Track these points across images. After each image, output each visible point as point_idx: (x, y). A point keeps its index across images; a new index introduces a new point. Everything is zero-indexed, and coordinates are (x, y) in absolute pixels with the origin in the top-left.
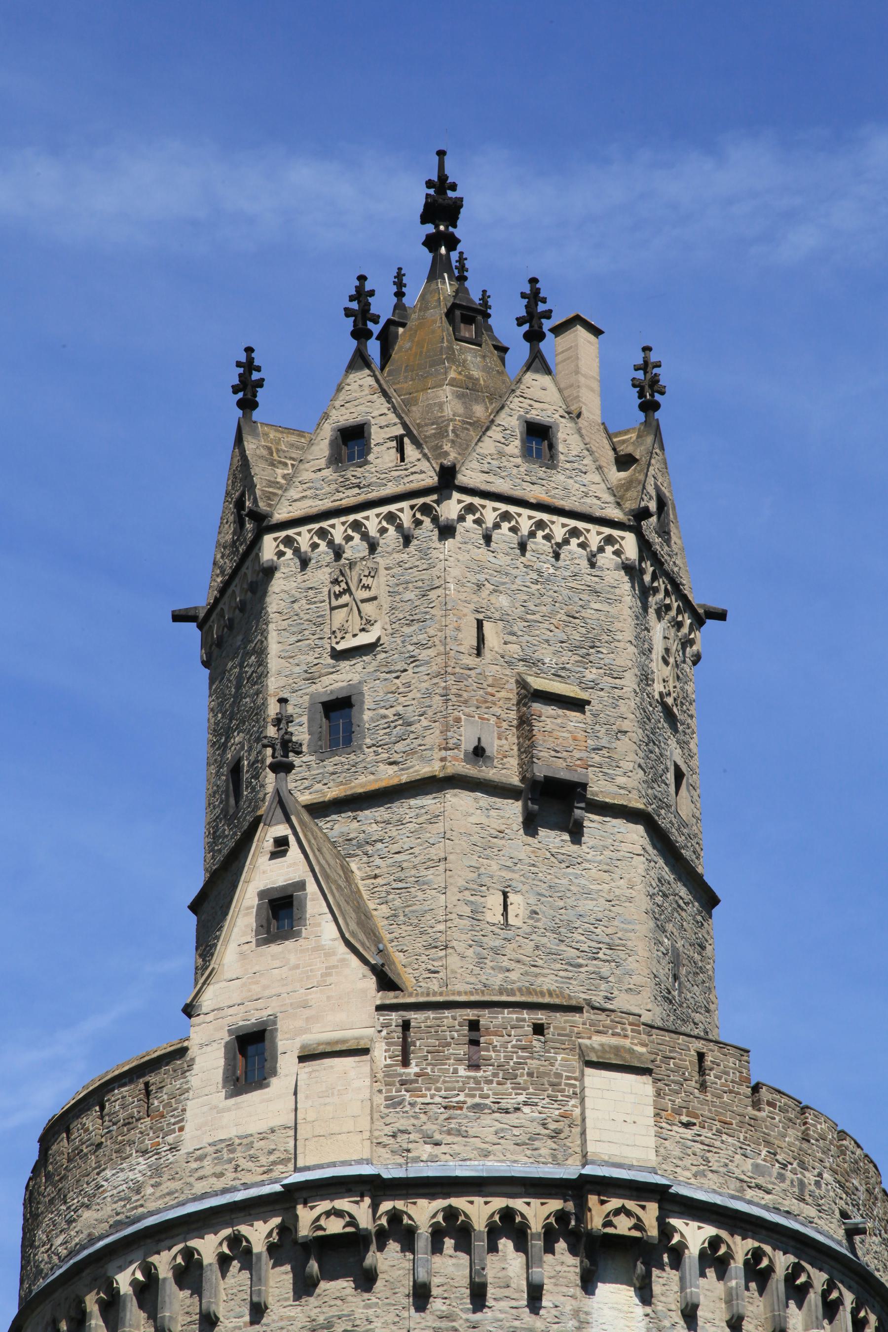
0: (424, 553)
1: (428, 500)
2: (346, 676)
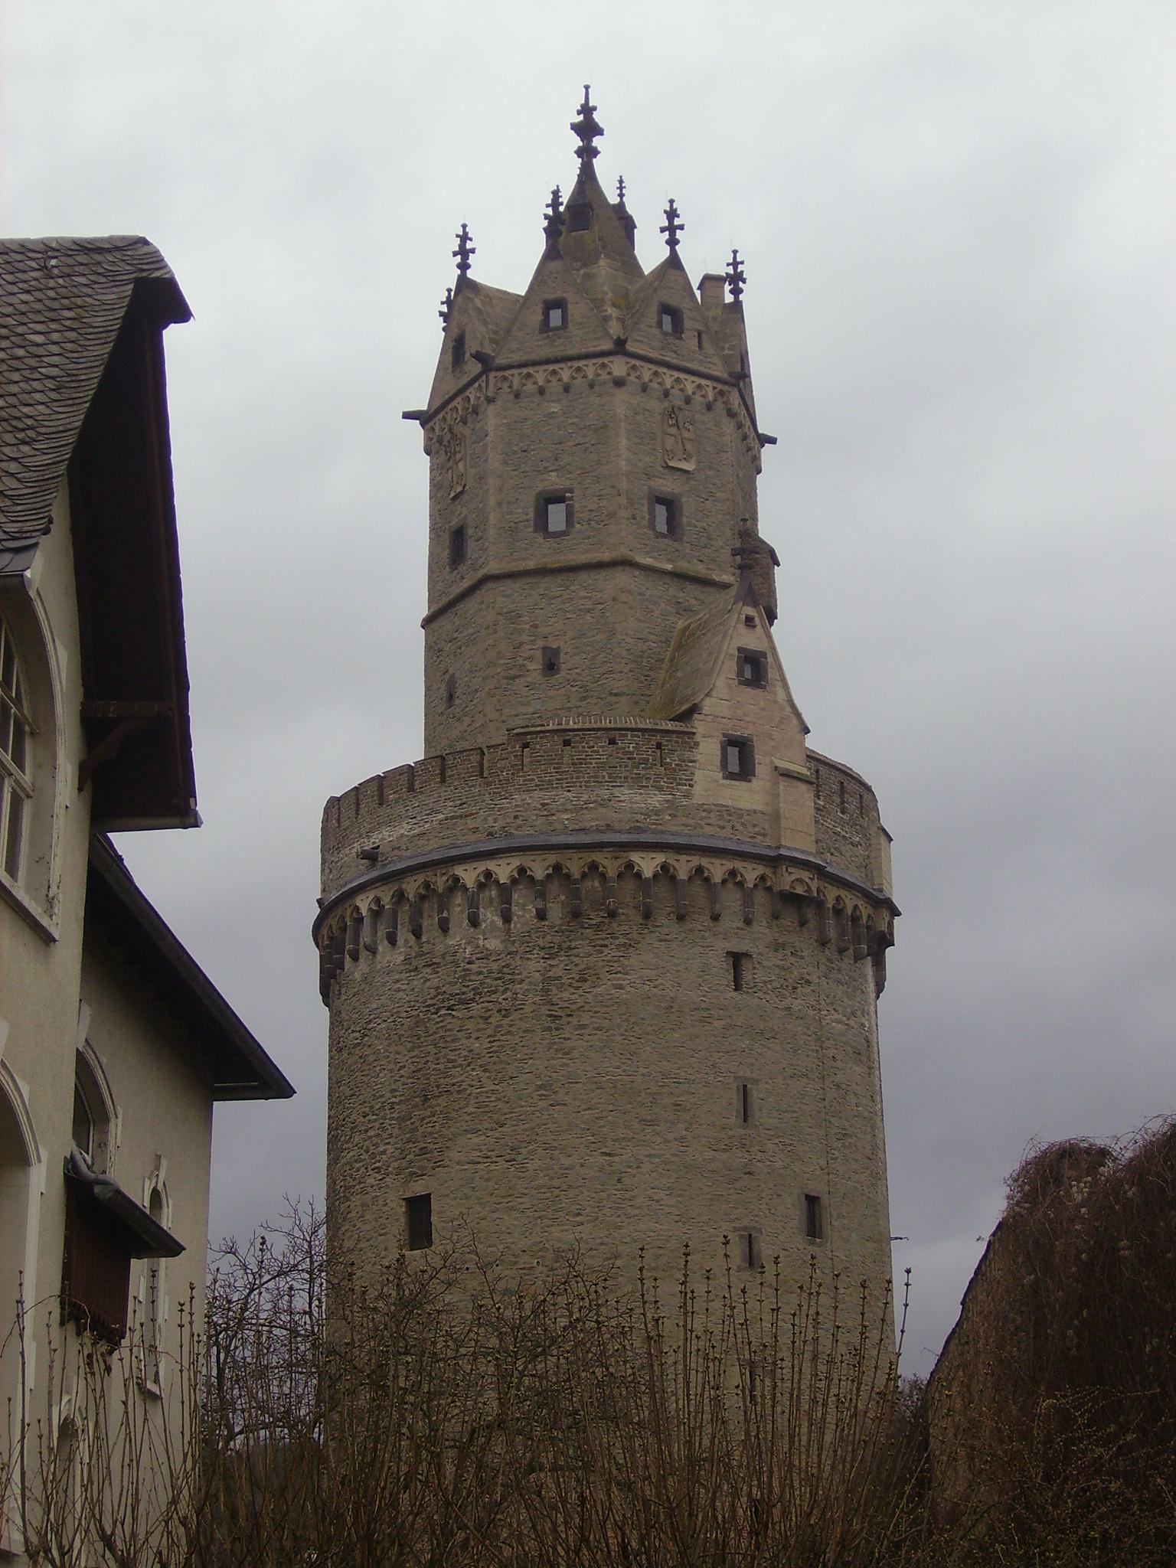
1: (725, 388)
2: (668, 485)
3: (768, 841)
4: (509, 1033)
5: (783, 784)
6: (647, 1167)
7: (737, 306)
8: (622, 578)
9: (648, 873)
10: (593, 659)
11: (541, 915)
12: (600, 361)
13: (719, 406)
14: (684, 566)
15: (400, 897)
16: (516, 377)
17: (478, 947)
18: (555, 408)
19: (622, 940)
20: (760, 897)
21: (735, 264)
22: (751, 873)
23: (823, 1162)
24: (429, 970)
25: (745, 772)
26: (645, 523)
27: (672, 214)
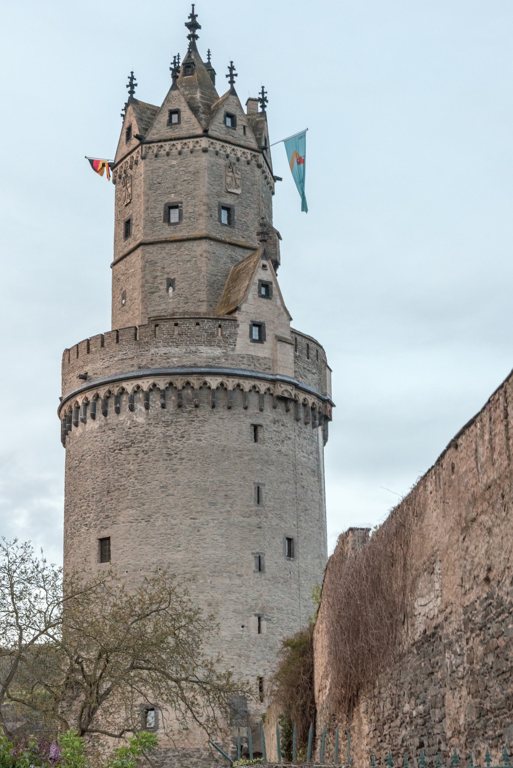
0: (252, 171)
1: (256, 154)
2: (229, 201)
3: (271, 372)
4: (147, 462)
5: (279, 344)
6: (211, 524)
7: (264, 113)
8: (204, 245)
9: (214, 386)
10: (191, 284)
11: (163, 406)
12: (195, 140)
13: (253, 162)
14: (234, 239)
15: (97, 397)
16: (155, 147)
17: (133, 421)
18: (174, 162)
19: (201, 418)
20: (267, 399)
21: (263, 93)
22: (263, 387)
23: (295, 523)
24: (111, 432)
25: (261, 339)
26: (216, 219)
27: (232, 68)
